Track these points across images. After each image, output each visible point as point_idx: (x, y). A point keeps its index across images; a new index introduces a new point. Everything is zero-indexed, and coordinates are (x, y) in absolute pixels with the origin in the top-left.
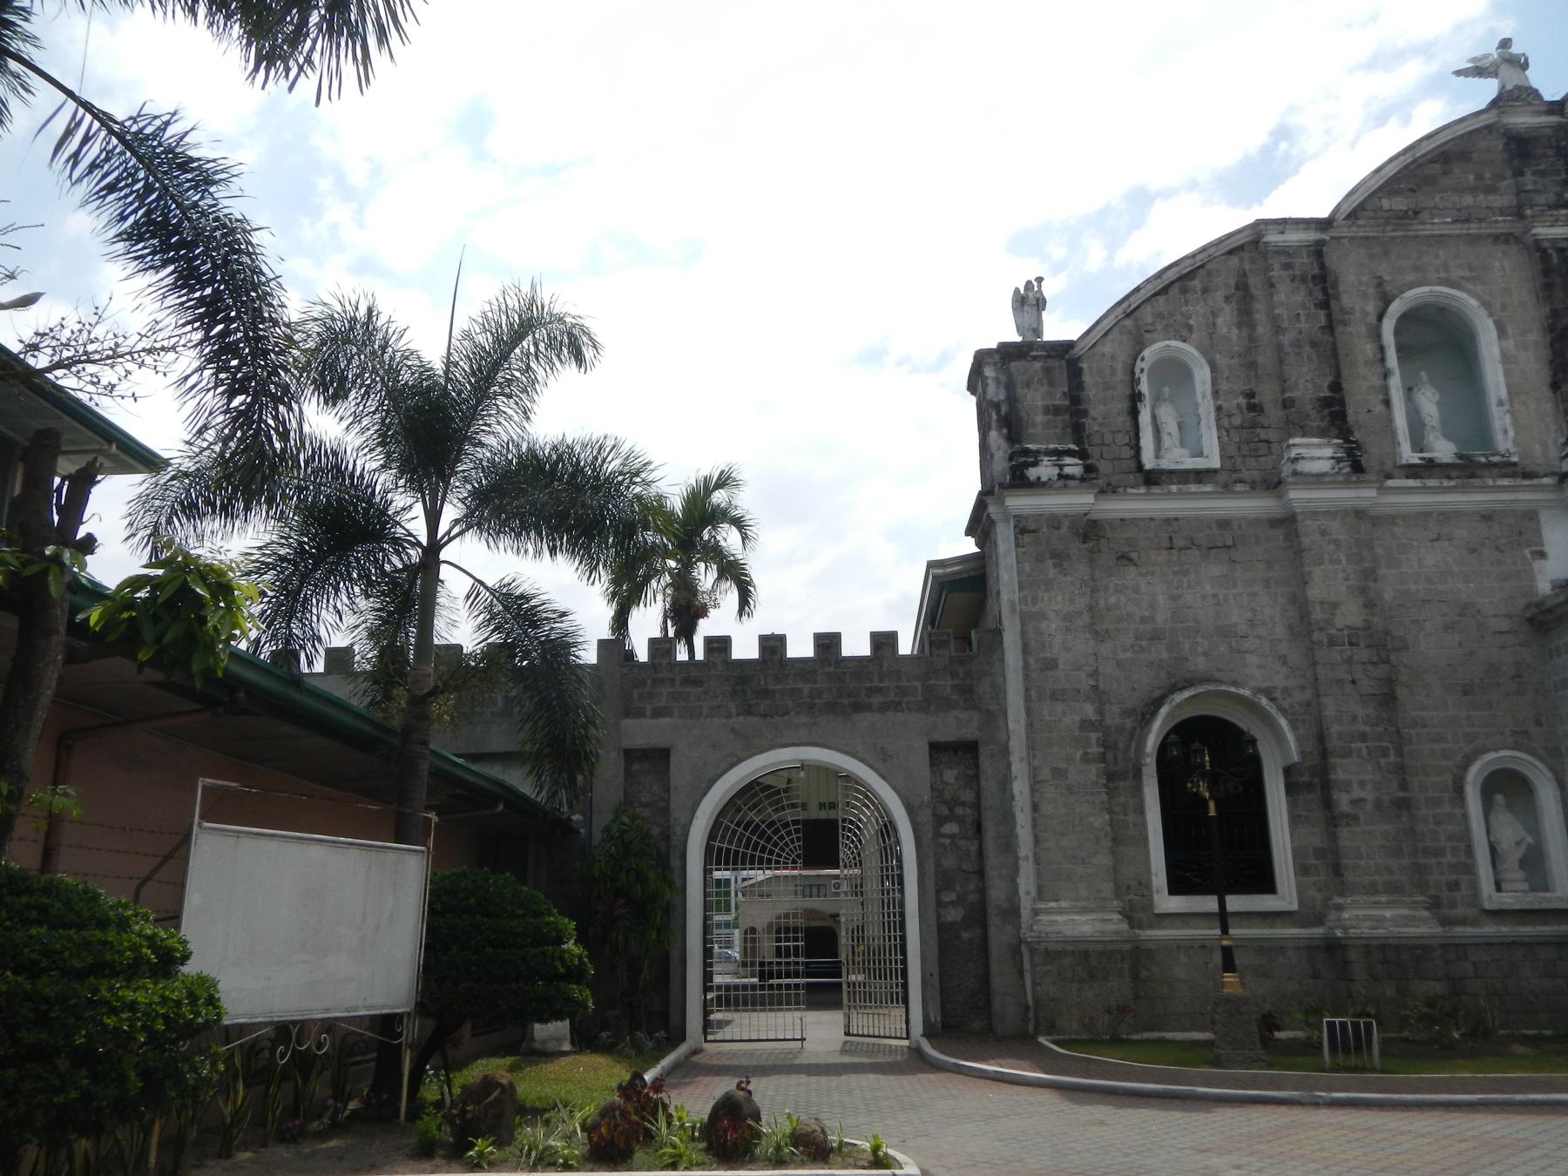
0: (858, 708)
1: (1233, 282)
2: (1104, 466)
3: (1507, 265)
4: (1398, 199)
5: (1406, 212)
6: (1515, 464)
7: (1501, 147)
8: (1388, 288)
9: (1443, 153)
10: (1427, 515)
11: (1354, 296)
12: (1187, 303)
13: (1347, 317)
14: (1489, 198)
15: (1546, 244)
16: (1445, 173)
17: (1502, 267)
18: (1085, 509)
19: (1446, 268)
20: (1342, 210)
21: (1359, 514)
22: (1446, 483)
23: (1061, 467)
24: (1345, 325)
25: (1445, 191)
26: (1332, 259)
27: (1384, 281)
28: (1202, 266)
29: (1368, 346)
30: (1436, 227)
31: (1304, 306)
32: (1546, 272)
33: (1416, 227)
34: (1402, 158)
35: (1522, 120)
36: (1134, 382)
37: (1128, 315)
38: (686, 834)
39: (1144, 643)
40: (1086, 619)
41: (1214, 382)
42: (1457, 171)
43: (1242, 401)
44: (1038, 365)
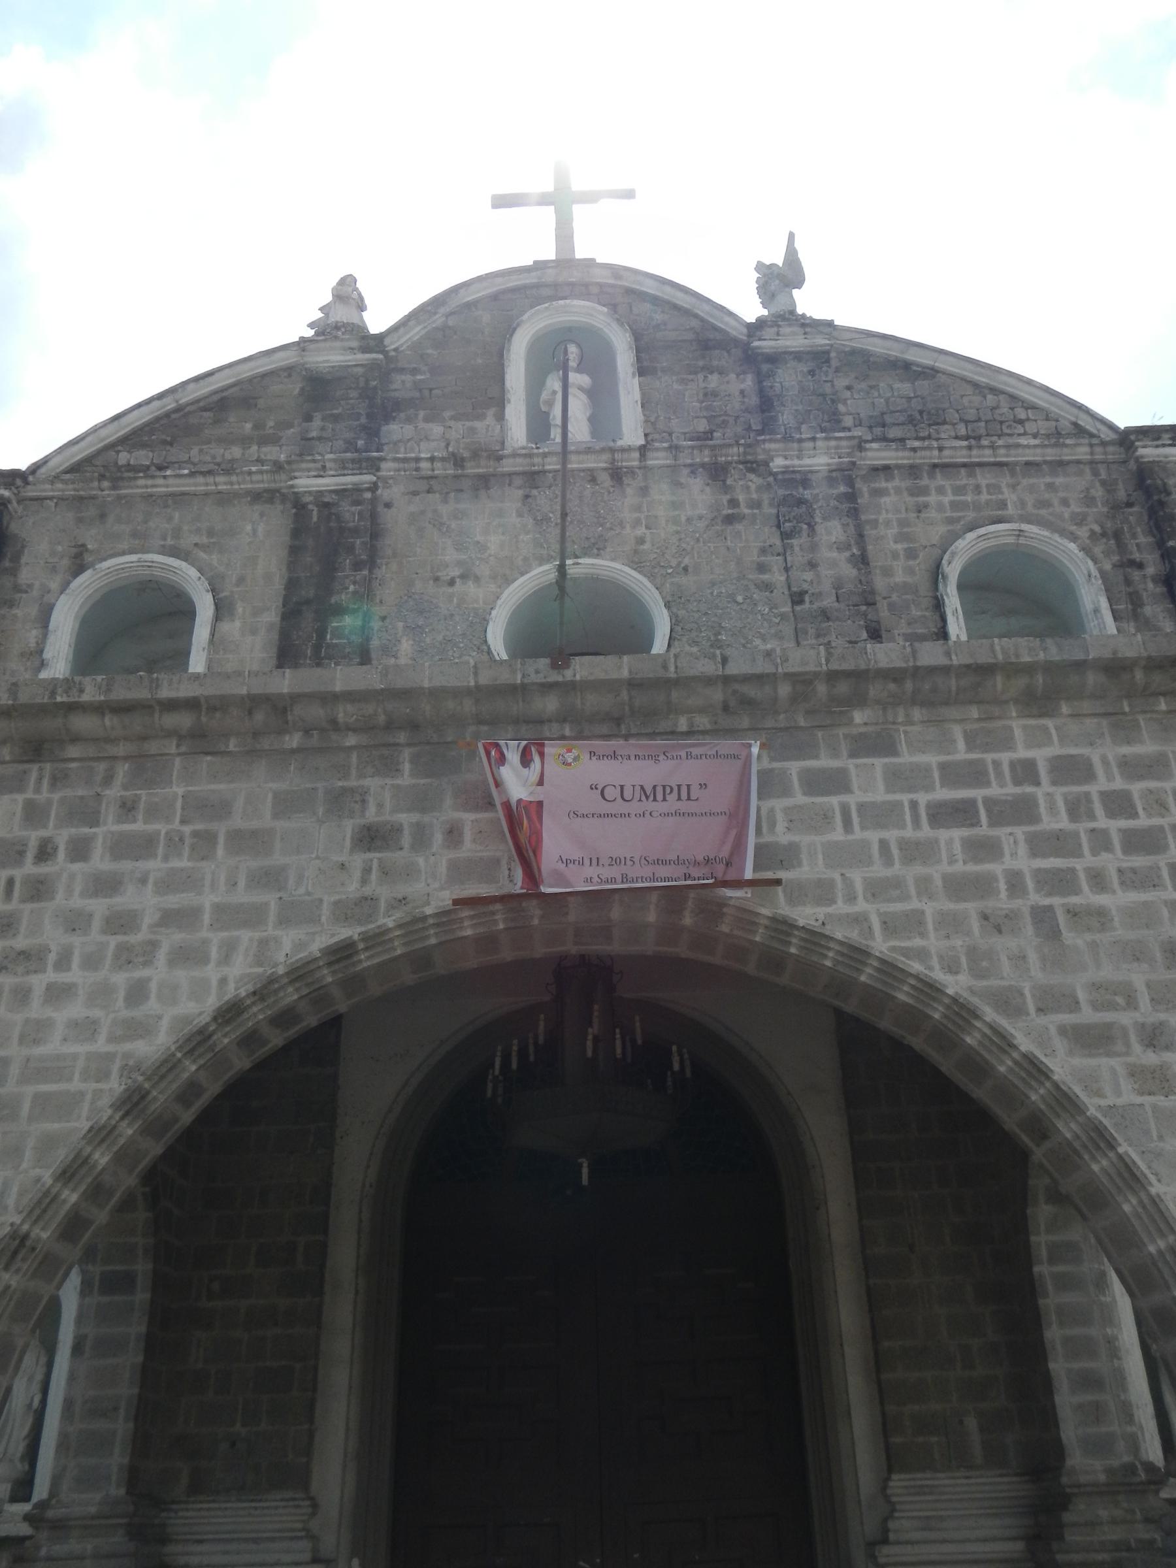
3: (261, 529)
4: (142, 453)
5: (148, 467)
7: (296, 391)
8: (88, 558)
13: (18, 596)
14: (264, 449)
15: (307, 499)
16: (217, 422)
17: (254, 531)
19: (177, 533)
20: (51, 464)
24: (11, 606)
25: (209, 442)
27: (87, 550)
29: (34, 632)
30: (171, 481)
32: (296, 533)
33: (141, 482)
34: (156, 404)
35: (331, 358)
42: (232, 420)
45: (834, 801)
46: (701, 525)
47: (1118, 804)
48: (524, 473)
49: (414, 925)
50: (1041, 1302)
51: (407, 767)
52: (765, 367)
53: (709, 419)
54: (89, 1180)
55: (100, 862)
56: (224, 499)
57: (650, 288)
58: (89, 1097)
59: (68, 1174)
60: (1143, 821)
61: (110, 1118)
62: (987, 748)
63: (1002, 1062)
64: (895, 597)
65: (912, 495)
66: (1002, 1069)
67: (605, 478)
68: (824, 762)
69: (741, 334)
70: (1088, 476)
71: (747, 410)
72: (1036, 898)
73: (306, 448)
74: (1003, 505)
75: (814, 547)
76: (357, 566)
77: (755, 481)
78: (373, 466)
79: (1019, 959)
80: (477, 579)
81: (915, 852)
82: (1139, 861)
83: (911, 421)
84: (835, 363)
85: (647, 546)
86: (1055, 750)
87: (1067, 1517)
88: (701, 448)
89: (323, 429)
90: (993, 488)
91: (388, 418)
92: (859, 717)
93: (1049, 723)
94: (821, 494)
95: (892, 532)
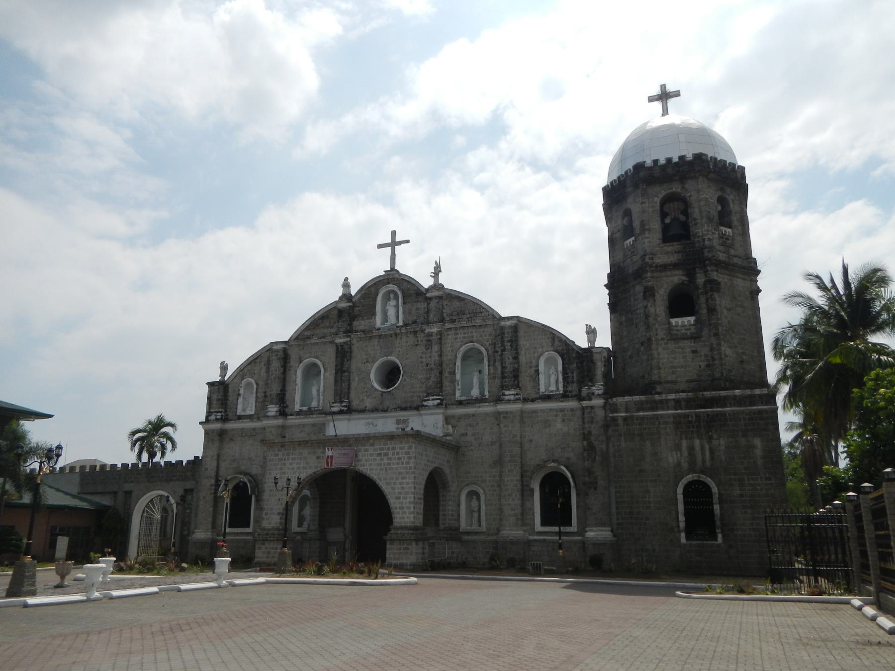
0: (171, 480)
1: (266, 359)
2: (230, 415)
4: (309, 332)
5: (310, 335)
6: (322, 410)
7: (336, 313)
8: (302, 359)
9: (323, 316)
10: (300, 425)
11: (293, 362)
12: (255, 366)
16: (322, 322)
18: (219, 428)
19: (317, 352)
21: (279, 426)
22: (301, 417)
23: (216, 416)
26: (290, 352)
28: (260, 355)
31: (279, 367)
32: (337, 353)
35: (344, 305)
36: (239, 390)
37: (241, 371)
38: (133, 511)
39: (232, 462)
40: (216, 457)
41: (257, 389)
43: (263, 394)
44: (217, 387)
45: (367, 453)
46: (411, 347)
47: (398, 453)
48: (378, 335)
49: (321, 469)
51: (321, 448)
52: (429, 301)
53: (417, 316)
55: (290, 461)
56: (325, 343)
57: (407, 279)
60: (400, 456)
62: (385, 445)
64: (447, 362)
65: (455, 335)
67: (394, 336)
68: (367, 447)
69: (424, 291)
70: (492, 328)
71: (425, 313)
72: (386, 466)
73: (336, 334)
74: (473, 337)
75: (431, 352)
76: (348, 361)
77: (422, 335)
78: (350, 336)
79: (383, 474)
80: (369, 362)
81: (375, 460)
82: (398, 461)
83: (458, 314)
84: (444, 298)
85: (400, 353)
86: (393, 446)
88: (411, 328)
89: (341, 325)
90: (472, 332)
91: (354, 320)
92: (371, 441)
93: (392, 441)
94: (435, 338)
95: (450, 345)
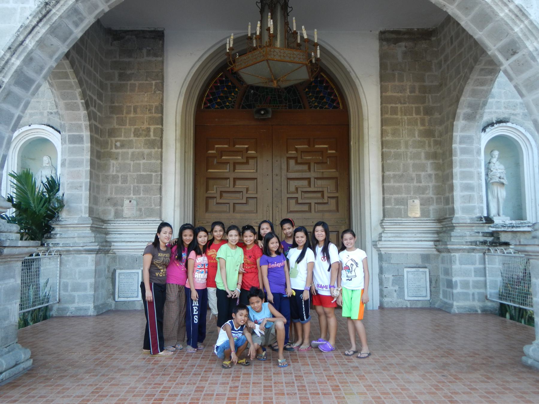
50: (454, 158)
54: (25, 54)
58: (19, 10)
59: (12, 50)
61: (31, 21)
63: (502, 10)
66: (502, 15)
87: (453, 234)
